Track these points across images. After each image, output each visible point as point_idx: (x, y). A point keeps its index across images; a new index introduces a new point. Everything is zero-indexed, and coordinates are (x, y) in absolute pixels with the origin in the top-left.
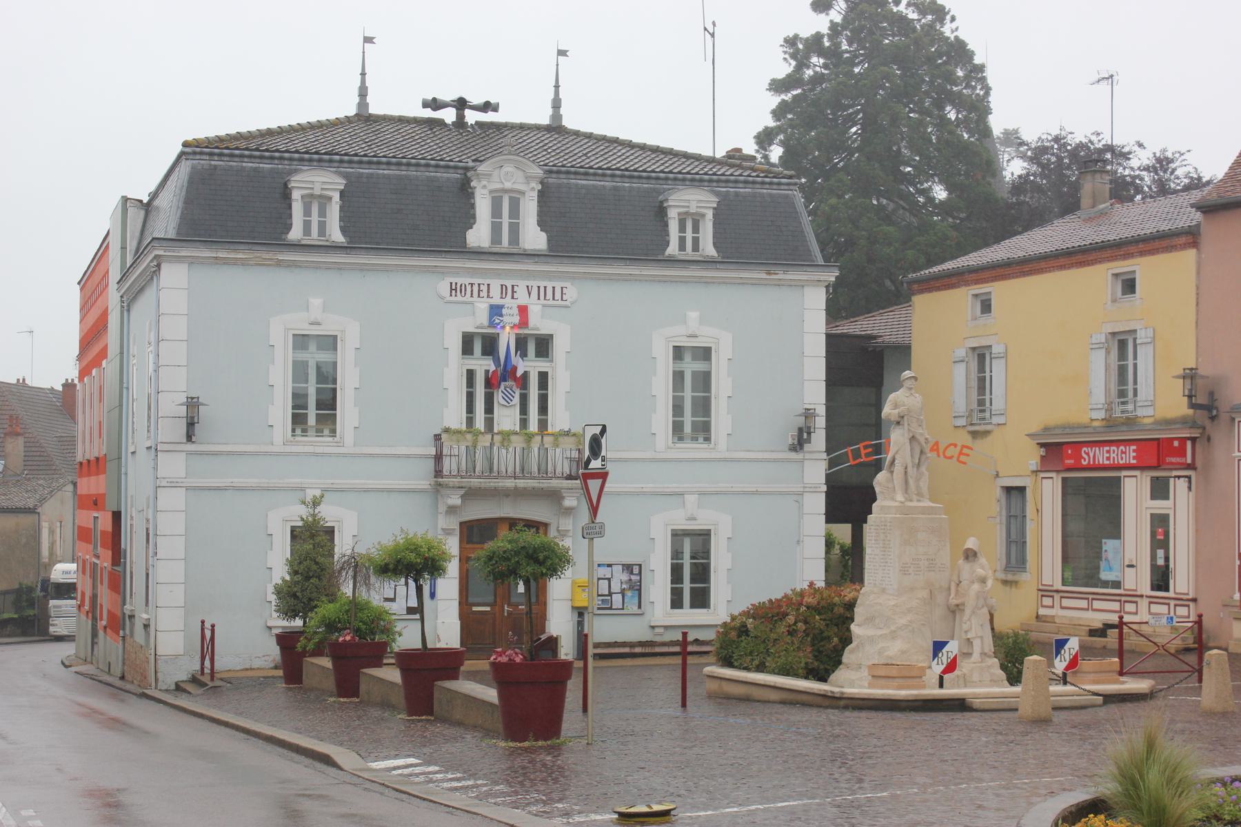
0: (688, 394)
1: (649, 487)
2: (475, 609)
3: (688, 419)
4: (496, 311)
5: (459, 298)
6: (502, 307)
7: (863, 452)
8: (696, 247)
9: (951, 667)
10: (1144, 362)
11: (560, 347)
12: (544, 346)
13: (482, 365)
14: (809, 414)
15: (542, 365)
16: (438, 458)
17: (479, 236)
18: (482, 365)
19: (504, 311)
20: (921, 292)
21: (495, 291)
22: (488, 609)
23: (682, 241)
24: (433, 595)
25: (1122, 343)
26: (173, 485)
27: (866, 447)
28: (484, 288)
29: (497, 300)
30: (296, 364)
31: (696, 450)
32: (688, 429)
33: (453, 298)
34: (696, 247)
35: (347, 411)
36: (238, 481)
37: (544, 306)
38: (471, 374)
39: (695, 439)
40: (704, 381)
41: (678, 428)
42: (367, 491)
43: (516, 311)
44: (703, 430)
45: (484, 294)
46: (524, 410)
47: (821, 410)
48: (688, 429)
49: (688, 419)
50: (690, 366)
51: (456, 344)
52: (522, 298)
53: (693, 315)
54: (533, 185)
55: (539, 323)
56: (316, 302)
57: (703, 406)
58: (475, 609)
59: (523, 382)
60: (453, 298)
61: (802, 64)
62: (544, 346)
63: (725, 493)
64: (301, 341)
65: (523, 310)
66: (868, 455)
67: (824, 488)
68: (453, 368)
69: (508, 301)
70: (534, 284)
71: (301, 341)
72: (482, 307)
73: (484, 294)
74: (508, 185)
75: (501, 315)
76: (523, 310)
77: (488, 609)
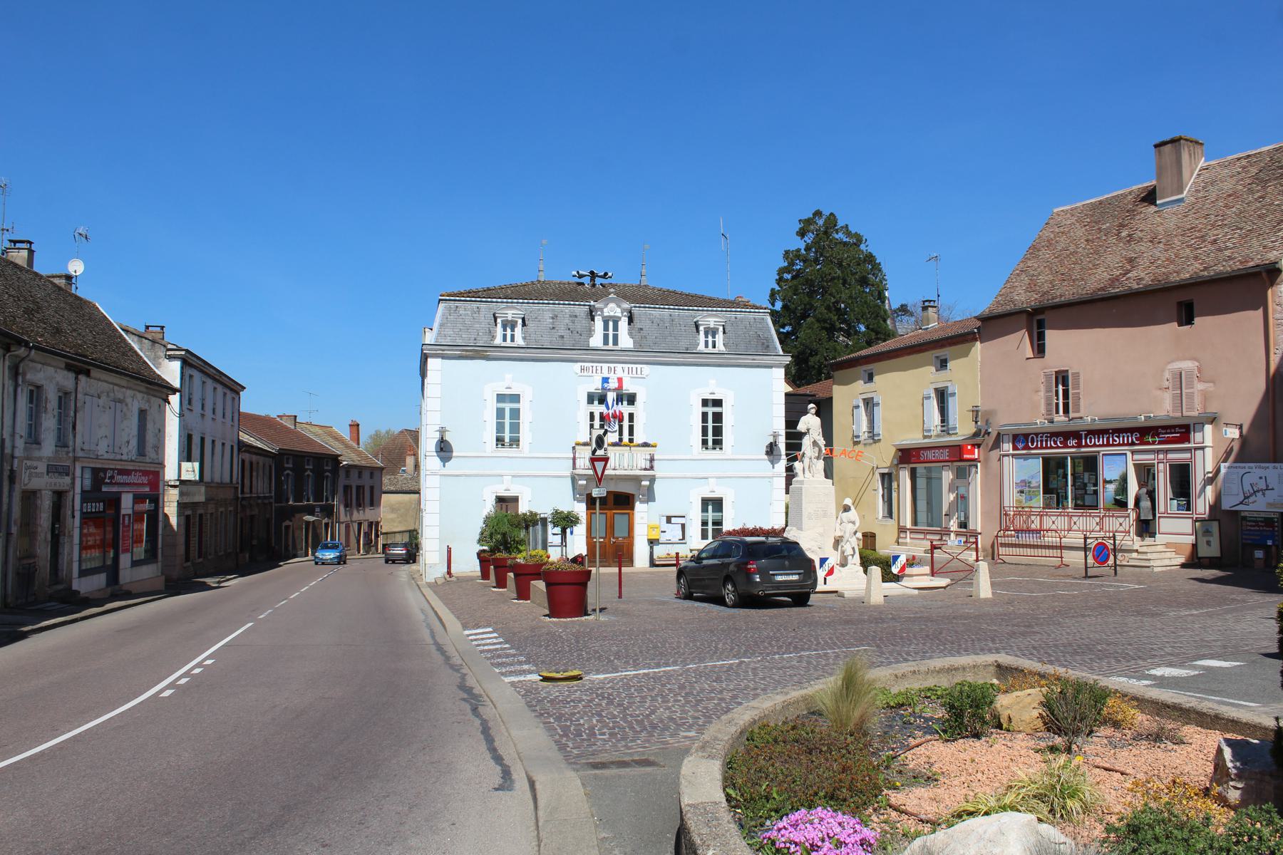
0: (710, 424)
1: (689, 474)
3: (710, 438)
4: (605, 380)
9: (831, 572)
10: (954, 405)
12: (631, 399)
14: (775, 435)
15: (630, 409)
16: (574, 459)
17: (596, 341)
18: (598, 409)
20: (837, 370)
23: (707, 343)
25: (942, 395)
26: (434, 474)
29: (606, 375)
30: (498, 409)
31: (716, 454)
32: (710, 443)
34: (714, 346)
35: (525, 435)
36: (468, 472)
38: (592, 415)
40: (718, 417)
41: (705, 442)
44: (718, 443)
46: (621, 433)
47: (783, 432)
48: (710, 443)
49: (710, 438)
50: (710, 410)
52: (619, 374)
53: (713, 382)
55: (629, 387)
57: (718, 431)
59: (621, 420)
61: (792, 264)
62: (631, 399)
65: (620, 380)
68: (584, 409)
69: (611, 375)
70: (626, 366)
71: (501, 398)
76: (620, 380)
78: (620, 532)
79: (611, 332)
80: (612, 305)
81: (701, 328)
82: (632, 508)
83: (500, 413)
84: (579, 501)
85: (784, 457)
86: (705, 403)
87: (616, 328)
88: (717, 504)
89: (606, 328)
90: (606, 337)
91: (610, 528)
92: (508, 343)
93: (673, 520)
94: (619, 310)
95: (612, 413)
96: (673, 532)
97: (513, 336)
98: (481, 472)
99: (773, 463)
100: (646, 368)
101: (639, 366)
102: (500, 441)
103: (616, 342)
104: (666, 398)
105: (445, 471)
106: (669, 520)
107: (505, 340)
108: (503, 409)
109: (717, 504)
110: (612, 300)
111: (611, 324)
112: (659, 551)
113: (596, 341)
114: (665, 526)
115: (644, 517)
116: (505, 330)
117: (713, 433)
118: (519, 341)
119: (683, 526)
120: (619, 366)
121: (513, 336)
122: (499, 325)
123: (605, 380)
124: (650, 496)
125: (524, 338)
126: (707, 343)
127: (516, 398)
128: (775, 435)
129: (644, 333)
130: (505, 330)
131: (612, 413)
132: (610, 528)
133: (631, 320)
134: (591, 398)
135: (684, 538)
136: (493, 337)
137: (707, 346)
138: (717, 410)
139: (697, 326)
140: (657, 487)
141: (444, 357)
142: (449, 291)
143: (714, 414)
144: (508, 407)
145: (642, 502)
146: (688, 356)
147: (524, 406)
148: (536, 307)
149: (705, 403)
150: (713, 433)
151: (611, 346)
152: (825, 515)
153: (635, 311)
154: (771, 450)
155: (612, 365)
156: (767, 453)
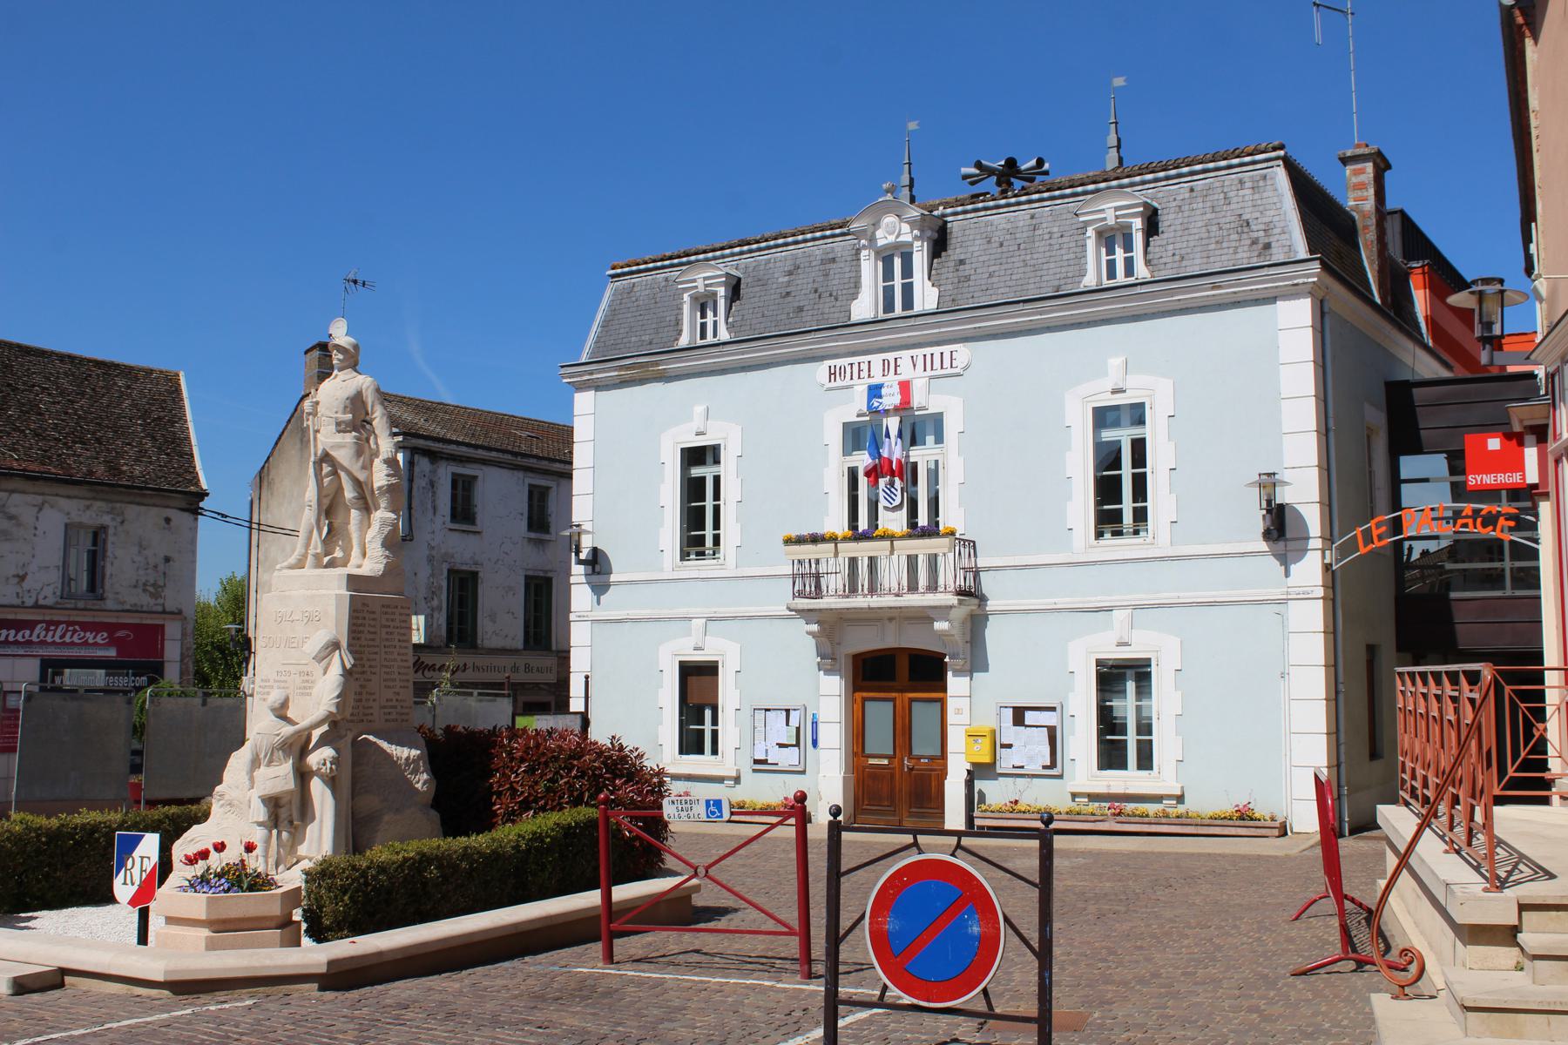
2: (872, 761)
3: (1127, 506)
4: (875, 391)
5: (839, 383)
6: (880, 387)
7: (1375, 533)
8: (1129, 271)
11: (951, 428)
13: (863, 460)
17: (864, 307)
19: (884, 391)
21: (877, 369)
22: (886, 762)
24: (815, 743)
27: (1378, 526)
28: (864, 367)
33: (833, 384)
34: (1129, 271)
37: (931, 378)
38: (853, 475)
39: (1136, 532)
42: (751, 618)
43: (897, 389)
45: (864, 374)
51: (835, 438)
52: (906, 372)
54: (916, 232)
58: (872, 761)
60: (833, 384)
63: (1170, 605)
65: (905, 387)
66: (1380, 538)
68: (833, 467)
70: (919, 352)
72: (861, 389)
73: (864, 374)
74: (891, 239)
75: (880, 397)
76: (905, 387)
77: (886, 762)
78: (923, 747)
79: (898, 282)
80: (890, 219)
82: (943, 688)
84: (828, 672)
85: (1315, 543)
86: (1103, 417)
87: (907, 272)
89: (888, 274)
90: (888, 293)
91: (903, 732)
92: (710, 339)
93: (1030, 717)
94: (906, 228)
95: (889, 461)
96: (1028, 748)
99: (1285, 560)
100: (963, 352)
101: (946, 349)
103: (908, 302)
104: (1008, 419)
105: (600, 614)
106: (1019, 716)
108: (702, 480)
110: (887, 209)
111: (897, 262)
112: (996, 792)
113: (864, 307)
114: (1010, 733)
115: (968, 708)
116: (703, 316)
117: (1117, 494)
118: (724, 335)
119: (1052, 731)
120: (905, 355)
122: (686, 308)
123: (875, 391)
124: (976, 662)
125: (730, 327)
126: (1111, 265)
129: (966, 269)
131: (889, 461)
132: (903, 732)
133: (939, 245)
134: (855, 436)
135: (1053, 765)
136: (680, 332)
138: (1136, 432)
140: (994, 634)
141: (598, 387)
142: (659, 255)
145: (957, 673)
146: (1058, 306)
147: (728, 470)
149: (1103, 417)
150: (1117, 494)
151: (898, 310)
153: (955, 225)
154: (1280, 525)
155: (890, 356)
156: (1267, 535)
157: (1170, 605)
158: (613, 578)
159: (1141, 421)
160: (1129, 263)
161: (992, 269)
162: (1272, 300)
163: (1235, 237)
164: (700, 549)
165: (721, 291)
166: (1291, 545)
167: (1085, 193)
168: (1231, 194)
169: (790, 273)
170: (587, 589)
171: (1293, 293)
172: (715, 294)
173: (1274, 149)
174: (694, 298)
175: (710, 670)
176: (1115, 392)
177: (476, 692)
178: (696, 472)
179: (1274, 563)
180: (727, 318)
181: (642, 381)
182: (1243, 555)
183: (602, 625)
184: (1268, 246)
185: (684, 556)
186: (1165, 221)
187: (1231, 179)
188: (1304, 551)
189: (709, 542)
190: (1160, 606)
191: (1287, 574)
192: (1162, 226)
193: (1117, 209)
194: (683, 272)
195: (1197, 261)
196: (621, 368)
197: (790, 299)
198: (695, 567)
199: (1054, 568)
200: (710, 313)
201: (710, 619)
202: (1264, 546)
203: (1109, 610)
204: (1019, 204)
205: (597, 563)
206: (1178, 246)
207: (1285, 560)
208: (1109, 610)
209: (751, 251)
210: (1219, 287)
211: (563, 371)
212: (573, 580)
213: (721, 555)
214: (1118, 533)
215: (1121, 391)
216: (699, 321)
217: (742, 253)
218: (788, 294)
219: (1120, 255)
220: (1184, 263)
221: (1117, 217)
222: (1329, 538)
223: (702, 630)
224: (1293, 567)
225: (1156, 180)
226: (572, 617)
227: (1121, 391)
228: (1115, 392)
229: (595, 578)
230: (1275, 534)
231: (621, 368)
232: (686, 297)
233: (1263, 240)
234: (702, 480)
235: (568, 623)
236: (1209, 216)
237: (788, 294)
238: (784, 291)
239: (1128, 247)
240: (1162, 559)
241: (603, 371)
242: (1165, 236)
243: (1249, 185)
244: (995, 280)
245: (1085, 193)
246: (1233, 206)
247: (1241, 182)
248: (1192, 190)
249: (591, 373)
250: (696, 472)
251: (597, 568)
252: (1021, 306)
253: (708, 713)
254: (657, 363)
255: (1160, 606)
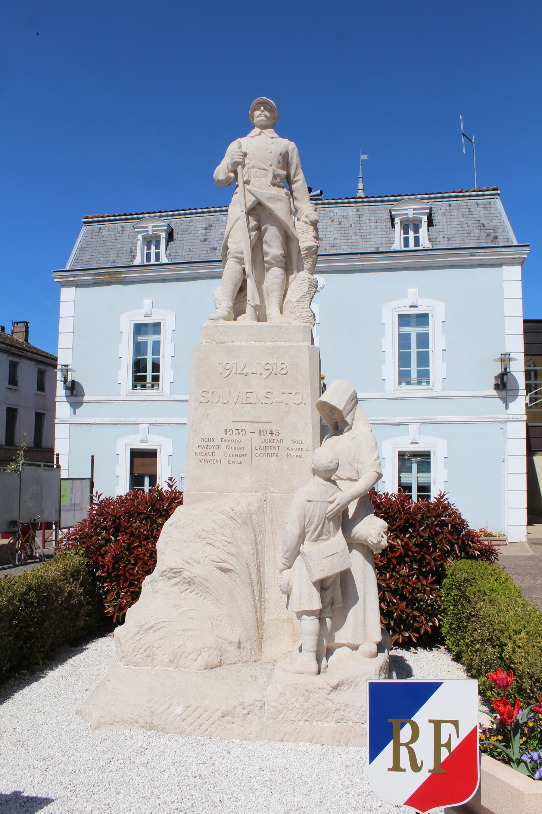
3: (414, 369)
14: (505, 359)
23: (406, 241)
26: (63, 423)
32: (414, 375)
39: (419, 383)
40: (423, 340)
44: (424, 376)
48: (414, 375)
49: (414, 369)
53: (412, 292)
56: (147, 302)
57: (424, 359)
63: (442, 423)
64: (139, 329)
67: (525, 418)
71: (139, 329)
81: (397, 220)
83: (139, 348)
85: (523, 392)
88: (423, 459)
92: (153, 261)
97: (158, 255)
98: (114, 420)
99: (506, 401)
102: (139, 380)
107: (148, 259)
109: (423, 459)
117: (414, 359)
118: (164, 259)
121: (158, 255)
122: (139, 243)
125: (168, 256)
126: (406, 241)
127: (156, 327)
128: (505, 359)
130: (149, 248)
136: (134, 257)
137: (406, 243)
138: (422, 329)
139: (393, 220)
141: (78, 285)
143: (419, 335)
144: (149, 339)
147: (166, 338)
148: (186, 220)
150: (414, 359)
152: (270, 443)
154: (503, 383)
157: (442, 423)
158: (85, 398)
159: (426, 324)
160: (417, 241)
161: (336, 236)
162: (501, 265)
163: (478, 231)
164: (143, 383)
165: (163, 235)
166: (509, 393)
167: (388, 201)
168: (473, 210)
169: (206, 229)
170: (67, 405)
171: (511, 263)
172: (159, 237)
173: (494, 190)
174: (144, 238)
175: (152, 454)
176: (411, 307)
177: (42, 464)
178: (141, 338)
179: (500, 403)
180: (166, 250)
181: (108, 283)
182: (483, 397)
183: (77, 426)
184: (496, 238)
185: (134, 387)
186: (436, 219)
187: (472, 202)
188: (517, 396)
189: (149, 379)
190: (436, 423)
191: (507, 408)
192: (435, 222)
193: (414, 209)
194: (137, 223)
195: (458, 242)
196: (96, 274)
197: (207, 242)
198: (140, 394)
199: (374, 401)
200: (153, 248)
201: (151, 424)
202: (495, 393)
203: (406, 424)
204: (349, 203)
205: (74, 389)
206: (446, 233)
207: (506, 401)
208: (406, 424)
209: (179, 215)
210: (474, 256)
211: (55, 274)
212: (57, 399)
213: (160, 388)
214: (409, 383)
215: (415, 306)
216: (146, 251)
217: (173, 215)
218: (205, 240)
219: (411, 235)
220: (450, 242)
221: (414, 214)
222: (529, 388)
223: (147, 430)
224: (510, 405)
225: (429, 198)
226: (56, 421)
227: (415, 306)
228: (411, 307)
229: (73, 398)
230: (501, 386)
231: (96, 274)
232: (140, 236)
233: (493, 234)
234: (146, 343)
235: (54, 425)
236: (461, 219)
237: (205, 240)
238: (203, 238)
239: (416, 231)
240: (437, 398)
241: (84, 275)
242: (437, 227)
243: (481, 206)
244: (338, 241)
245: (388, 201)
246: (474, 216)
247: (477, 204)
248: (450, 205)
249: (75, 276)
250: (141, 338)
251: (75, 392)
252: (359, 256)
253: (147, 480)
254: (121, 273)
255: (436, 423)
